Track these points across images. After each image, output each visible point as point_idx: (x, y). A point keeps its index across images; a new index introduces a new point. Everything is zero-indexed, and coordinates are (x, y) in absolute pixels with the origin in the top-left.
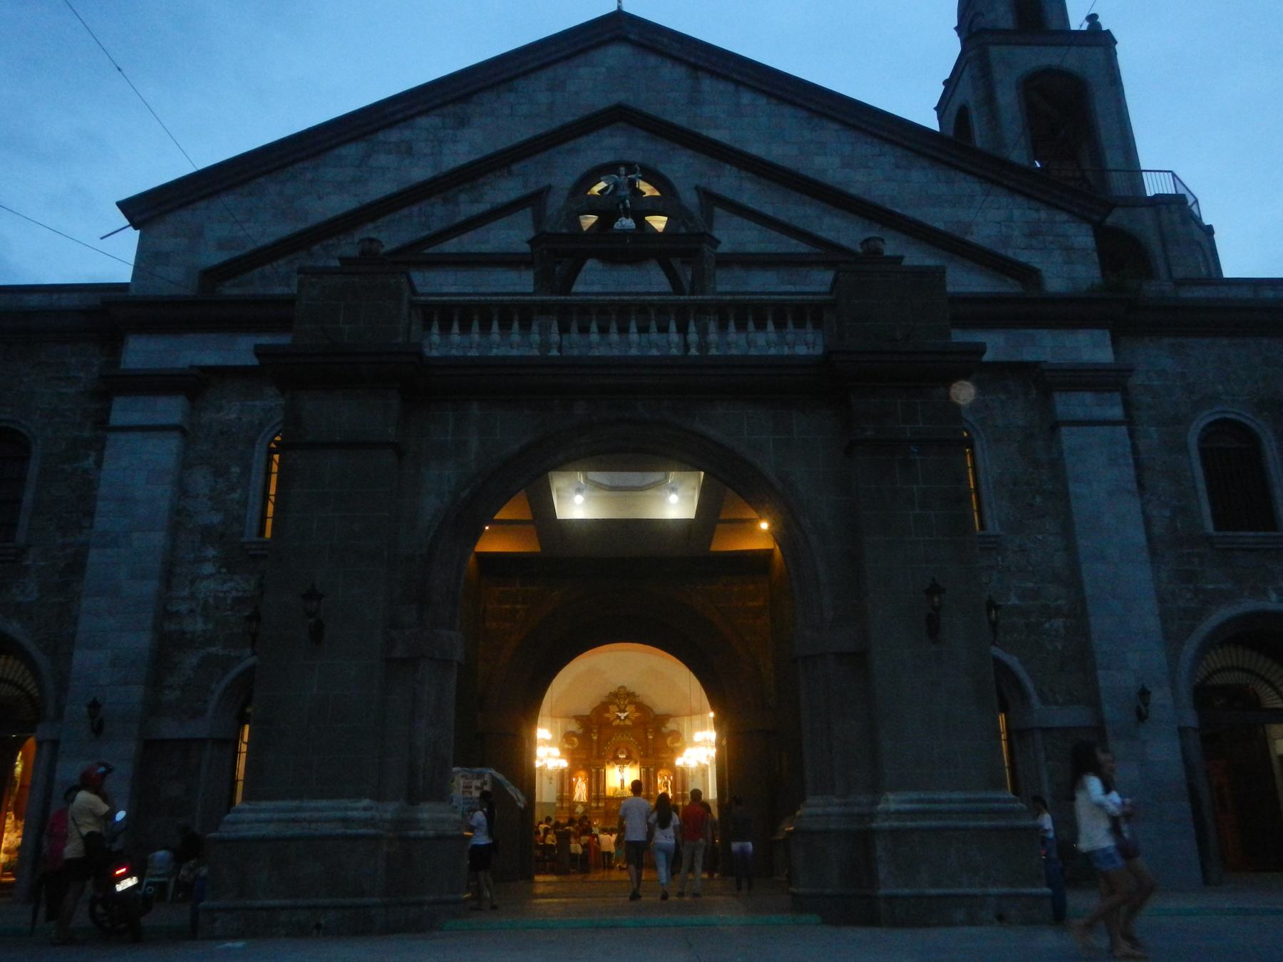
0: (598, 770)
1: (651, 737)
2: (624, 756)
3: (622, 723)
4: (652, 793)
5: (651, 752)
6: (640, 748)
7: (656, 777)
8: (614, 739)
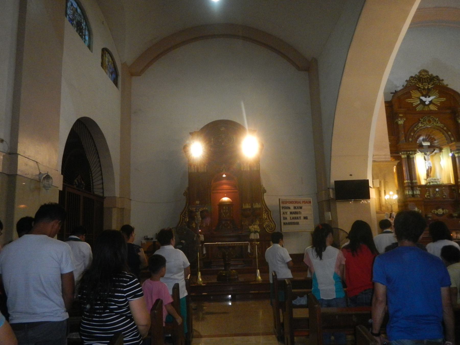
3: (426, 109)
6: (450, 133)
8: (420, 125)
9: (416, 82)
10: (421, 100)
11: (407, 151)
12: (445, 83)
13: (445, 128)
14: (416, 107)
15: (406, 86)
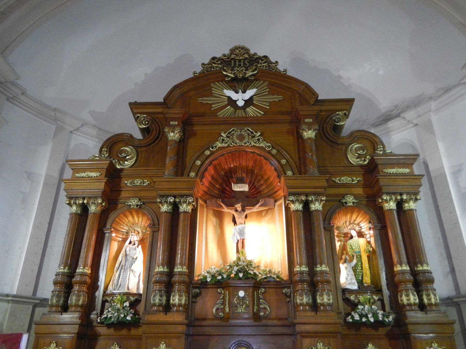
0: (175, 206)
1: (309, 134)
2: (245, 188)
3: (240, 113)
4: (324, 268)
5: (313, 169)
6: (284, 161)
7: (329, 229)
9: (220, 66)
10: (229, 98)
11: (168, 196)
12: (281, 67)
13: (274, 152)
14: (217, 113)
15: (202, 73)
